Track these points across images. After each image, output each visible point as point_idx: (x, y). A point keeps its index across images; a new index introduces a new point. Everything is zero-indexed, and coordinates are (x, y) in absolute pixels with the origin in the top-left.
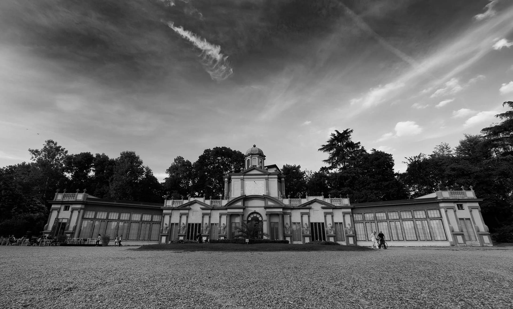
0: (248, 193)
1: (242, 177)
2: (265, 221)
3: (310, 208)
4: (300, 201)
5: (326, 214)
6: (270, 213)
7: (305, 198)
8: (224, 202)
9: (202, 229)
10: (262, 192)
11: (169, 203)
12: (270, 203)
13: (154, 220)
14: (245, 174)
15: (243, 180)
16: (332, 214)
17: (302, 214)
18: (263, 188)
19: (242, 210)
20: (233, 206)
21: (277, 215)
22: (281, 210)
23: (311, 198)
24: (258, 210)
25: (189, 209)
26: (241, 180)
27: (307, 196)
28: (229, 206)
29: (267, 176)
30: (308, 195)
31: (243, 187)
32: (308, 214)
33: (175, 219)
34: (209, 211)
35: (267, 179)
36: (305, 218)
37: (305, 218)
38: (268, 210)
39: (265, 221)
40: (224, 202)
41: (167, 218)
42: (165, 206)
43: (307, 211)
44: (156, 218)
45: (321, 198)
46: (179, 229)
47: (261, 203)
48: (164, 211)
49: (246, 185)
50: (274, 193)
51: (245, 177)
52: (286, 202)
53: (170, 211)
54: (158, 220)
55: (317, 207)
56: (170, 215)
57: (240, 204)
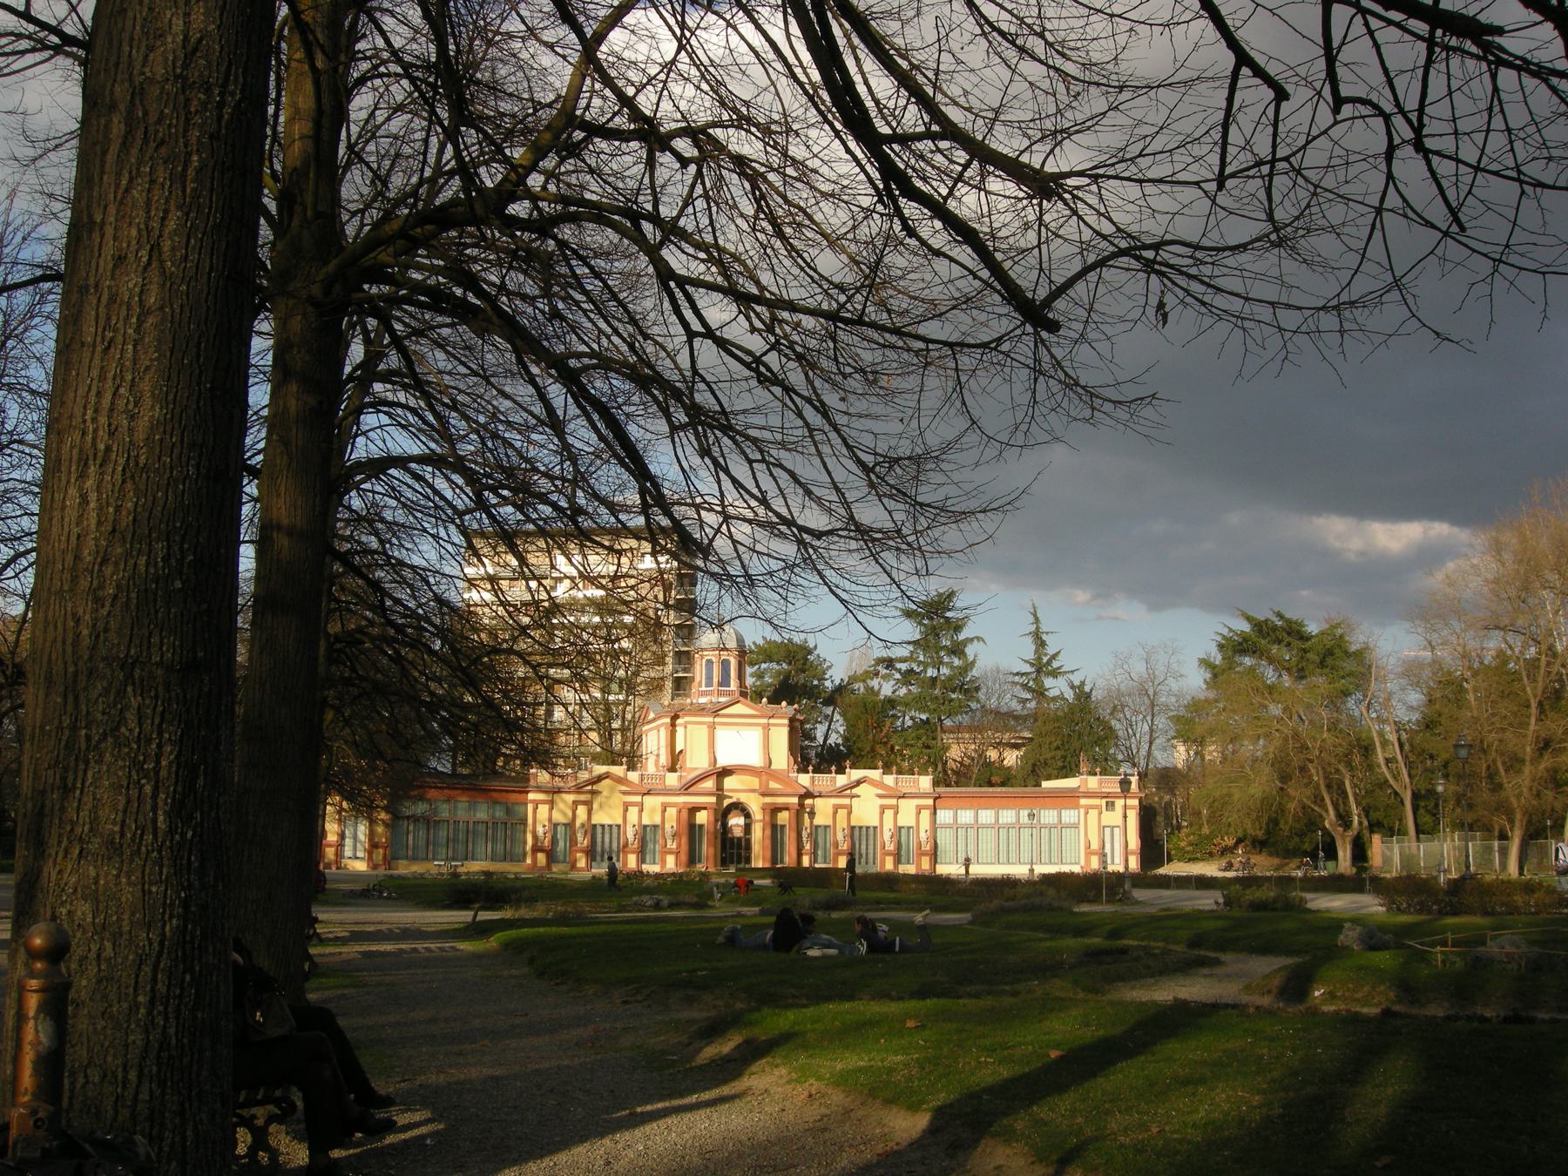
0: (722, 762)
10: (756, 760)
15: (712, 727)
23: (856, 774)
24: (743, 798)
25: (593, 793)
26: (709, 727)
27: (848, 770)
35: (767, 728)
38: (768, 800)
43: (846, 801)
45: (875, 774)
47: (754, 782)
50: (781, 758)
51: (717, 720)
52: (804, 779)
57: (709, 784)
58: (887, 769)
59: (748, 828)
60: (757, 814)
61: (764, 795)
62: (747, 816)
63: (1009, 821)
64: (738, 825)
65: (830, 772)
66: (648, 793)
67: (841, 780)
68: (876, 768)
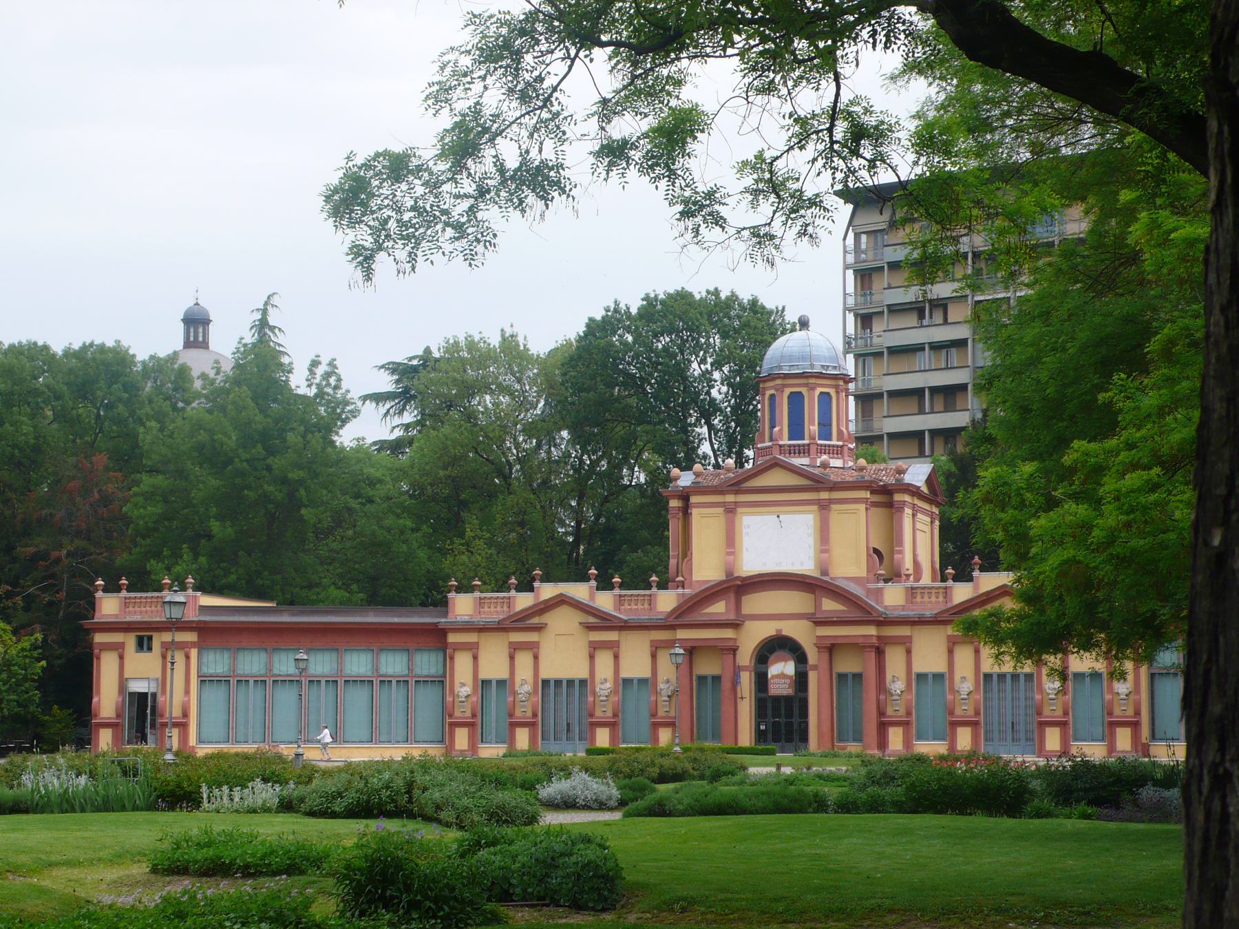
1: (730, 498)
2: (815, 668)
3: (539, 628)
4: (651, 600)
5: (594, 647)
6: (828, 642)
7: (970, 579)
8: (666, 601)
9: (451, 699)
10: (802, 561)
11: (463, 606)
12: (830, 605)
13: (418, 671)
14: (736, 486)
15: (731, 510)
16: (613, 646)
17: (515, 648)
18: (811, 541)
19: (728, 633)
20: (688, 619)
21: (856, 646)
22: (871, 631)
23: (547, 591)
27: (976, 574)
28: (682, 616)
29: (824, 495)
30: (982, 569)
31: (731, 540)
32: (533, 648)
33: (494, 663)
34: (612, 636)
35: (824, 506)
36: (524, 660)
37: (524, 661)
39: (815, 668)
40: (666, 601)
41: (462, 663)
42: (450, 618)
44: (427, 663)
45: (580, 591)
46: (510, 699)
48: (452, 638)
49: (744, 531)
53: (471, 638)
54: (433, 671)
55: (563, 623)
56: (473, 649)
57: (719, 608)
58: (604, 584)
59: (801, 680)
60: (812, 656)
61: (819, 623)
62: (800, 657)
63: (219, 670)
64: (782, 676)
65: (649, 587)
66: (625, 626)
67: (523, 601)
68: (584, 578)
